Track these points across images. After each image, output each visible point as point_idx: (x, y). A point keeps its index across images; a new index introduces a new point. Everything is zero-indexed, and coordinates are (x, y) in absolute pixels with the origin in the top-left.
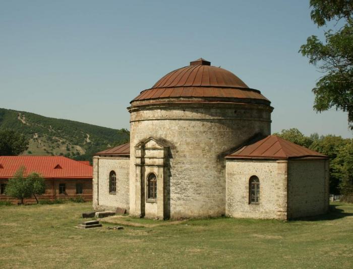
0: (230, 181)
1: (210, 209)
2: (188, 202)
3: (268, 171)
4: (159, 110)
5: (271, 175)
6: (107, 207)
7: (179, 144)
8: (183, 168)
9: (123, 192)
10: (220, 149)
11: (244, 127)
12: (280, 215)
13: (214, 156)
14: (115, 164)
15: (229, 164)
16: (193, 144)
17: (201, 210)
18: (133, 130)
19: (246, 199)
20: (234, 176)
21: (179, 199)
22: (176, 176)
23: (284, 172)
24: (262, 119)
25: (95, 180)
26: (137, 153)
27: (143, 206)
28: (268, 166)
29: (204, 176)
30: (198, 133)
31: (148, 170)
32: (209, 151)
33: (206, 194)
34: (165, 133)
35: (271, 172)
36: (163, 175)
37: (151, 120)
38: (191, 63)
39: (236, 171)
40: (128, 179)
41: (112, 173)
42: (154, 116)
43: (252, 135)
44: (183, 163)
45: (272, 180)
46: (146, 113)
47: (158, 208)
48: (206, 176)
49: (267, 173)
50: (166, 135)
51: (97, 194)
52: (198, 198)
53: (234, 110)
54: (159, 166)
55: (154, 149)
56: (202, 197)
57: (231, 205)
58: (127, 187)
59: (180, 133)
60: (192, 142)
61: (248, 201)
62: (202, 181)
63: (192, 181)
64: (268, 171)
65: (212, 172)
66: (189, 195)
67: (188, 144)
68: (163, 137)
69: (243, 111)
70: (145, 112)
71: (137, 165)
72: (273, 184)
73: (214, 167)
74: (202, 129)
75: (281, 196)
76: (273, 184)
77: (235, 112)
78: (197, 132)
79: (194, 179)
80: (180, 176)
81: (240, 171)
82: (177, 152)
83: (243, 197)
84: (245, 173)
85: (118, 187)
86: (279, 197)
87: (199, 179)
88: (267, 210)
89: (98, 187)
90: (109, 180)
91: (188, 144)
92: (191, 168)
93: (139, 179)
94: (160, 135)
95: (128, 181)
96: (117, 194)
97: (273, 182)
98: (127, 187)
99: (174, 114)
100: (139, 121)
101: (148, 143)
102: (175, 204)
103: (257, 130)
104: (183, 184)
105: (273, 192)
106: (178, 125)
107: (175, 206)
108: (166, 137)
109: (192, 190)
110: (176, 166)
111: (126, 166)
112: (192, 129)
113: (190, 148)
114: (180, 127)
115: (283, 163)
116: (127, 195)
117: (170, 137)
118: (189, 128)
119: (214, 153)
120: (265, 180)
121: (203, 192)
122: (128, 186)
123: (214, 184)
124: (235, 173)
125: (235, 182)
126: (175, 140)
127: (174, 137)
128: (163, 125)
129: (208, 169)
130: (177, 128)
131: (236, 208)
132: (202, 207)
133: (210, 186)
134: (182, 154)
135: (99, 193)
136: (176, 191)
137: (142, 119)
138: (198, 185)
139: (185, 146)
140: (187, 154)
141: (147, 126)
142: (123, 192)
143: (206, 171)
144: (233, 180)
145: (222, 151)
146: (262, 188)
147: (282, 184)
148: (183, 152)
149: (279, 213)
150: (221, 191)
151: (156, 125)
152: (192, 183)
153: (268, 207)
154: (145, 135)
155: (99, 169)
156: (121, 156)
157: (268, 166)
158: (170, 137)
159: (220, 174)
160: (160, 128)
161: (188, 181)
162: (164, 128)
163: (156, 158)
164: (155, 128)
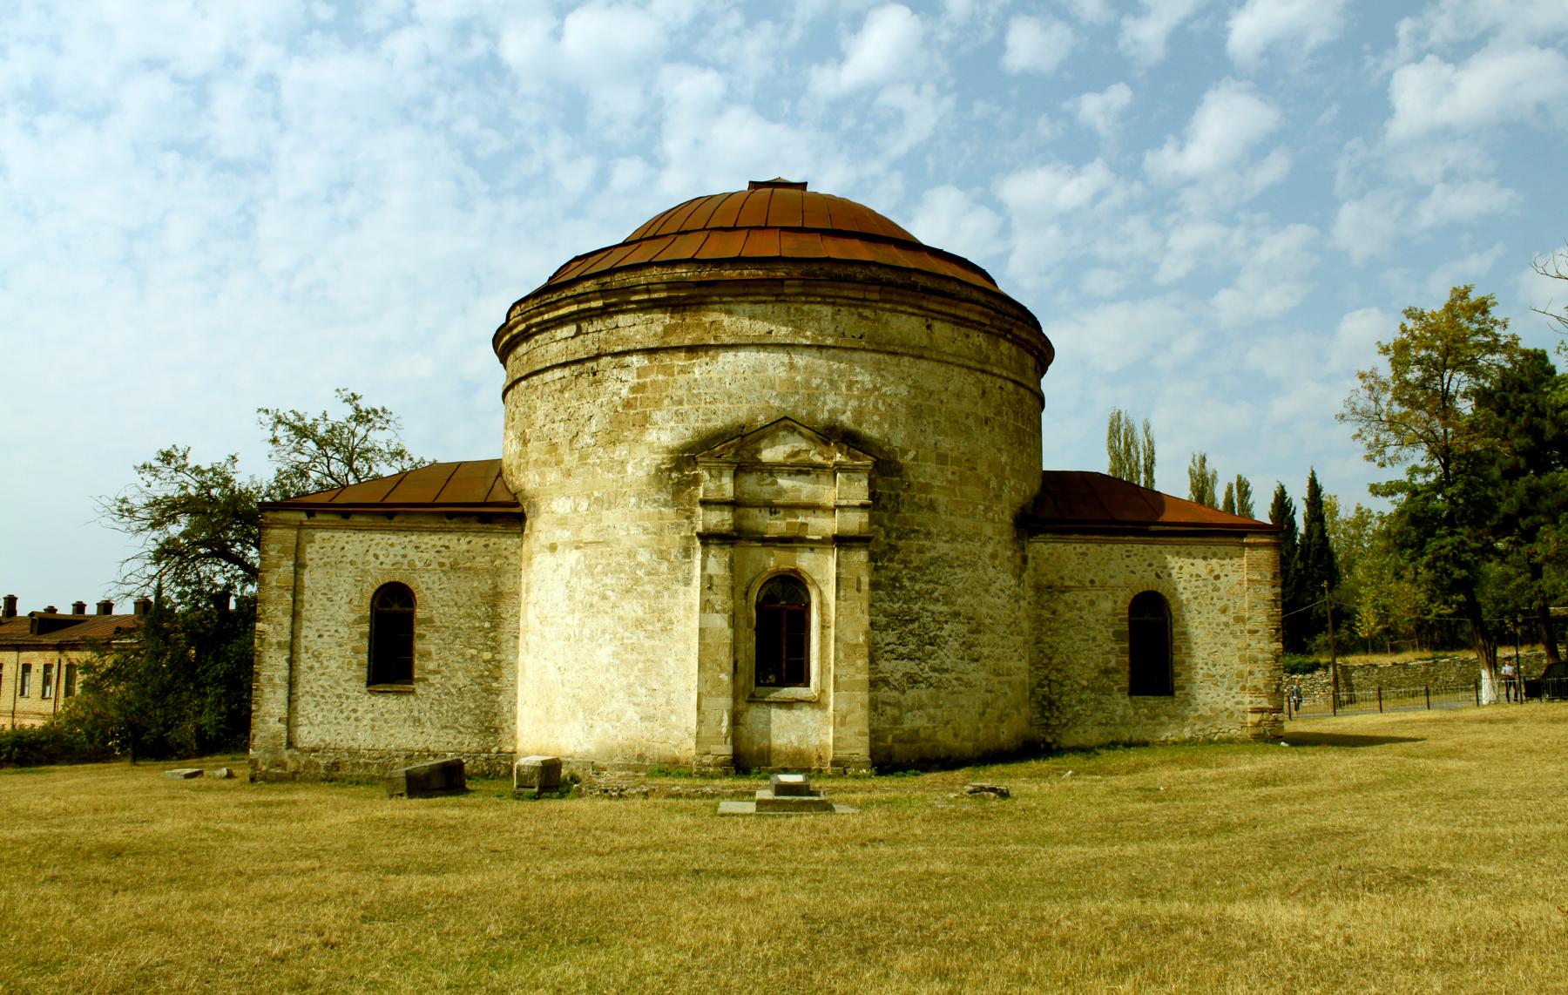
0: (1047, 615)
2: (943, 694)
4: (827, 311)
5: (1216, 589)
7: (911, 455)
8: (928, 555)
12: (1258, 724)
13: (1008, 517)
14: (412, 554)
16: (957, 461)
19: (1117, 677)
20: (1066, 596)
21: (913, 680)
22: (902, 587)
23: (1269, 576)
25: (271, 629)
30: (971, 422)
34: (854, 403)
35: (1217, 577)
36: (865, 579)
39: (1071, 579)
40: (496, 621)
44: (928, 535)
45: (1220, 604)
47: (841, 721)
49: (1200, 583)
51: (282, 694)
52: (971, 677)
54: (842, 541)
57: (1051, 703)
58: (487, 655)
59: (917, 413)
60: (955, 453)
61: (1126, 684)
62: (984, 611)
66: (948, 664)
67: (942, 459)
68: (846, 419)
72: (1224, 619)
75: (1260, 656)
76: (1224, 619)
78: (967, 416)
79: (959, 601)
81: (1090, 576)
83: (1107, 672)
84: (1112, 582)
85: (427, 655)
86: (1254, 660)
90: (366, 628)
91: (942, 459)
92: (952, 554)
95: (494, 628)
96: (419, 688)
97: (1224, 611)
98: (487, 655)
99: (895, 333)
100: (692, 350)
102: (898, 705)
104: (926, 618)
105: (1225, 645)
107: (896, 712)
110: (901, 543)
111: (482, 562)
112: (953, 404)
113: (950, 476)
115: (1266, 545)
116: (489, 691)
118: (944, 397)
124: (1067, 583)
125: (1068, 615)
126: (899, 438)
127: (891, 426)
130: (903, 390)
131: (1077, 715)
132: (983, 714)
134: (920, 497)
135: (300, 690)
136: (901, 650)
138: (974, 624)
139: (930, 468)
140: (941, 499)
142: (461, 680)
143: (991, 572)
144: (1061, 608)
147: (1264, 618)
148: (926, 488)
149: (1256, 718)
152: (956, 614)
155: (307, 578)
156: (450, 516)
158: (880, 425)
160: (831, 382)
161: (945, 609)
162: (850, 386)
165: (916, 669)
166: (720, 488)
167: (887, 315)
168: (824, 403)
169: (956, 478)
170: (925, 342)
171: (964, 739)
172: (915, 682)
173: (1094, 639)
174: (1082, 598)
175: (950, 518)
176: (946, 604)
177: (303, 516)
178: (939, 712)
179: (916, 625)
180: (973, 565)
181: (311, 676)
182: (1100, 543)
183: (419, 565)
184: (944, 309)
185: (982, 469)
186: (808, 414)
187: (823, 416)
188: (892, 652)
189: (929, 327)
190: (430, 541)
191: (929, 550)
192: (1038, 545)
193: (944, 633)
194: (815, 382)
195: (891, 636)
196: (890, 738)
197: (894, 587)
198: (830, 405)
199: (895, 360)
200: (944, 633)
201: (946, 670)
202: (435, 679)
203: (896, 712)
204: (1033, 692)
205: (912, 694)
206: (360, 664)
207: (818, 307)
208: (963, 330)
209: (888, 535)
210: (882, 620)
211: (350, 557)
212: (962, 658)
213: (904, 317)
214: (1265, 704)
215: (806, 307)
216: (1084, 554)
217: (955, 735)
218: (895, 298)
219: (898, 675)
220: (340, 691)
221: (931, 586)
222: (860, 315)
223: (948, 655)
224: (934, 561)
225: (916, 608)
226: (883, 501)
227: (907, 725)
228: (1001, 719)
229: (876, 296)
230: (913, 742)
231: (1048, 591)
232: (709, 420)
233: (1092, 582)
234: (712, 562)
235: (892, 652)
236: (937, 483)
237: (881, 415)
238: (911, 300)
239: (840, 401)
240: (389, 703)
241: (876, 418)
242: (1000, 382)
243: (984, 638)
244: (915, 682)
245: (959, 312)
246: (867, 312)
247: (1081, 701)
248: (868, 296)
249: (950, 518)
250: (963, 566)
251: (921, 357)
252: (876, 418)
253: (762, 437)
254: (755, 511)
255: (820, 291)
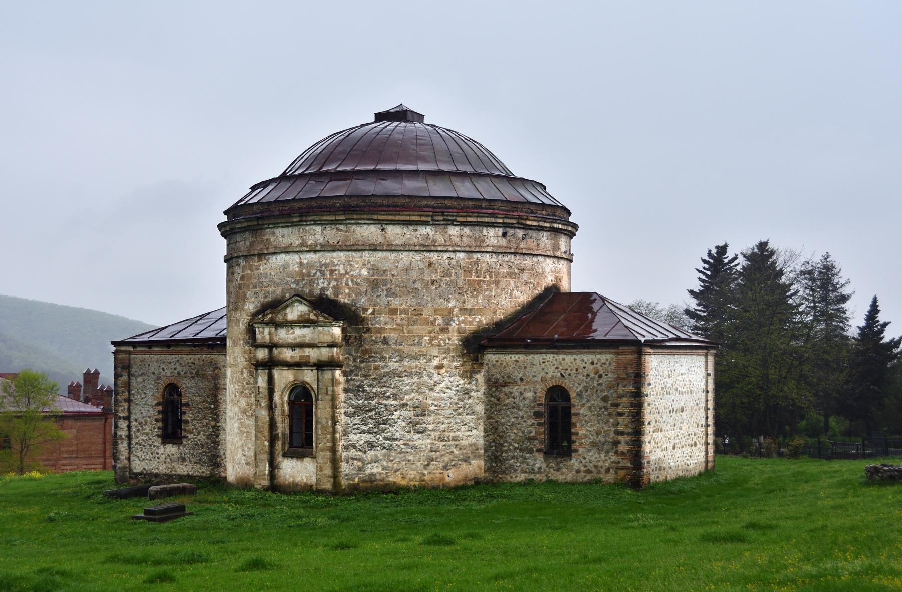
1: (445, 468)
3: (592, 375)
4: (318, 229)
6: (156, 475)
7: (370, 311)
9: (202, 437)
10: (471, 323)
11: (522, 271)
13: (455, 340)
15: (491, 357)
16: (405, 311)
17: (426, 472)
18: (242, 278)
20: (506, 389)
21: (371, 445)
22: (364, 391)
24: (558, 254)
26: (258, 336)
27: (273, 466)
28: (592, 363)
29: (432, 389)
31: (284, 377)
32: (444, 330)
33: (437, 434)
34: (334, 283)
35: (601, 376)
37: (297, 252)
38: (376, 115)
41: (172, 389)
42: (303, 245)
43: (540, 290)
44: (383, 358)
46: (284, 236)
48: (438, 388)
50: (337, 290)
52: (417, 443)
53: (500, 231)
55: (304, 322)
56: (429, 441)
57: (496, 457)
58: (213, 423)
60: (404, 306)
62: (429, 402)
63: (404, 401)
64: (592, 375)
65: (452, 379)
66: (397, 435)
68: (329, 293)
69: (520, 233)
70: (279, 232)
71: (258, 365)
73: (456, 368)
74: (427, 278)
77: (504, 235)
79: (407, 397)
80: (374, 390)
81: (520, 375)
82: (368, 330)
83: (530, 439)
86: (622, 433)
87: (421, 397)
88: (590, 466)
89: (129, 427)
92: (400, 369)
93: (264, 403)
94: (322, 289)
95: (216, 408)
96: (185, 442)
98: (213, 423)
101: (288, 310)
103: (549, 280)
106: (369, 266)
107: (360, 464)
108: (336, 294)
109: (404, 424)
110: (363, 365)
114: (374, 269)
117: (349, 295)
119: (455, 334)
120: (585, 395)
121: (431, 427)
122: (217, 420)
123: (455, 407)
125: (507, 401)
127: (356, 295)
128: (326, 265)
129: (442, 371)
130: (364, 272)
131: (511, 467)
133: (448, 412)
136: (363, 427)
137: (272, 251)
138: (419, 411)
140: (392, 336)
141: (285, 266)
143: (436, 377)
145: (473, 327)
146: (577, 414)
148: (380, 330)
149: (622, 473)
150: (472, 424)
151: (310, 265)
153: (593, 459)
154: (280, 289)
157: (592, 363)
159: (469, 383)
162: (332, 272)
163: (311, 345)
164: (309, 273)
165: (374, 439)
166: (263, 337)
167: (354, 227)
168: (318, 284)
169: (405, 322)
170: (381, 240)
171: (410, 480)
172: (373, 446)
173: (522, 417)
174: (515, 390)
175: (398, 347)
176: (396, 399)
177: (131, 349)
178: (390, 465)
179: (373, 413)
180: (420, 374)
181: (138, 434)
182: (526, 354)
183: (183, 373)
184: (390, 218)
185: (427, 312)
186: (310, 291)
187: (317, 292)
188: (357, 429)
189: (383, 230)
190: (187, 358)
191: (383, 368)
192: (489, 356)
193: (393, 417)
194: (313, 272)
195: (357, 420)
196: (356, 480)
197: (359, 391)
198: (321, 286)
199: (359, 254)
200: (393, 417)
201: (396, 439)
202: (190, 436)
203: (360, 464)
204: (486, 450)
205: (371, 453)
206: (159, 428)
207: (314, 227)
208: (411, 228)
209: (354, 360)
210: (351, 410)
211: (152, 370)
212: (409, 432)
213: (365, 227)
214: (629, 465)
215: (307, 228)
216: (517, 361)
217: (403, 478)
218: (355, 217)
219: (361, 443)
220: (151, 443)
221: (384, 389)
222: (337, 229)
223: (398, 429)
224: (387, 374)
225: (373, 403)
226: (352, 340)
227: (368, 472)
228: (445, 468)
229: (343, 218)
230: (372, 482)
231: (495, 385)
232: (265, 297)
233: (521, 379)
234: (260, 379)
235: (357, 429)
236: (389, 326)
237: (349, 289)
238: (365, 216)
239: (326, 283)
240: (171, 449)
241: (347, 291)
242: (447, 255)
243: (431, 419)
244: (373, 446)
245: (402, 218)
246: (341, 227)
247: (513, 457)
248: (338, 218)
249: (398, 347)
250: (411, 375)
251: (376, 250)
252: (347, 291)
253: (287, 306)
254: (285, 349)
255: (310, 218)
